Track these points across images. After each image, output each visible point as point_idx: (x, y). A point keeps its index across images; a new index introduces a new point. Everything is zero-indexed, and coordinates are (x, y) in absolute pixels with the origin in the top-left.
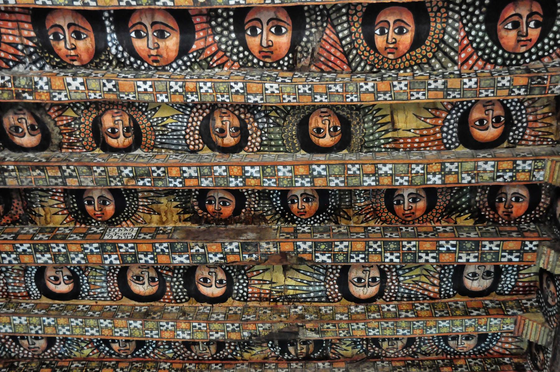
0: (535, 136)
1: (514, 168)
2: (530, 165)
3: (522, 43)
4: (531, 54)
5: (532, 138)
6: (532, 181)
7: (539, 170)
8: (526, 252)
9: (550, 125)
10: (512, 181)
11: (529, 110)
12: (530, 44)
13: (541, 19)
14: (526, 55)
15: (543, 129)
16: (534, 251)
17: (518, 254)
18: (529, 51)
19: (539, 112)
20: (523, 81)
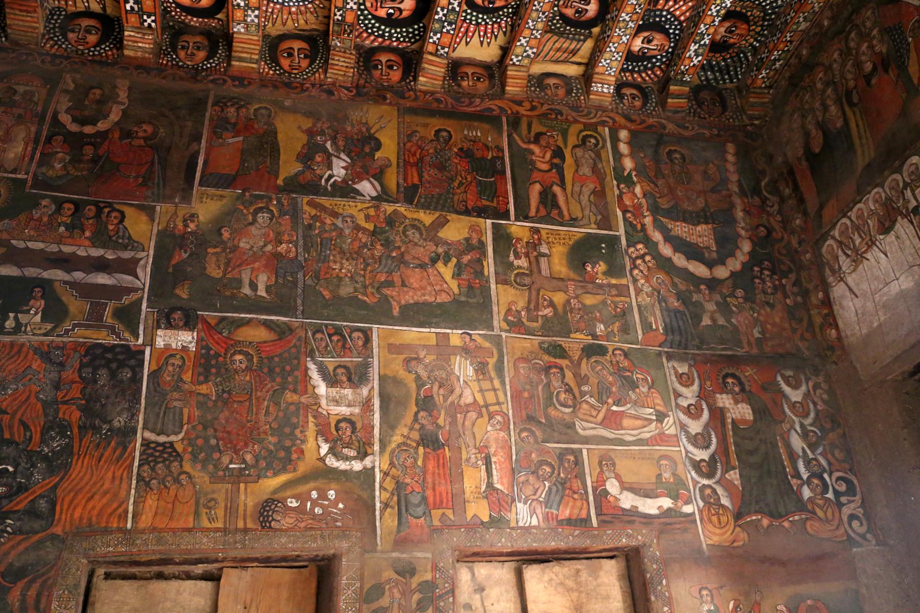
0: (272, 13)
1: (250, 8)
2: (253, 21)
3: (375, 4)
4: (362, 11)
5: (270, 10)
6: (233, 21)
7: (247, 28)
8: (141, 17)
9: (284, 24)
10: (233, 5)
11: (303, 8)
12: (372, 11)
13: (394, 17)
14: (362, 7)
15: (279, 18)
16: (142, 24)
17: (136, 9)
18: (366, 9)
19: (300, 16)
20: (350, 18)
